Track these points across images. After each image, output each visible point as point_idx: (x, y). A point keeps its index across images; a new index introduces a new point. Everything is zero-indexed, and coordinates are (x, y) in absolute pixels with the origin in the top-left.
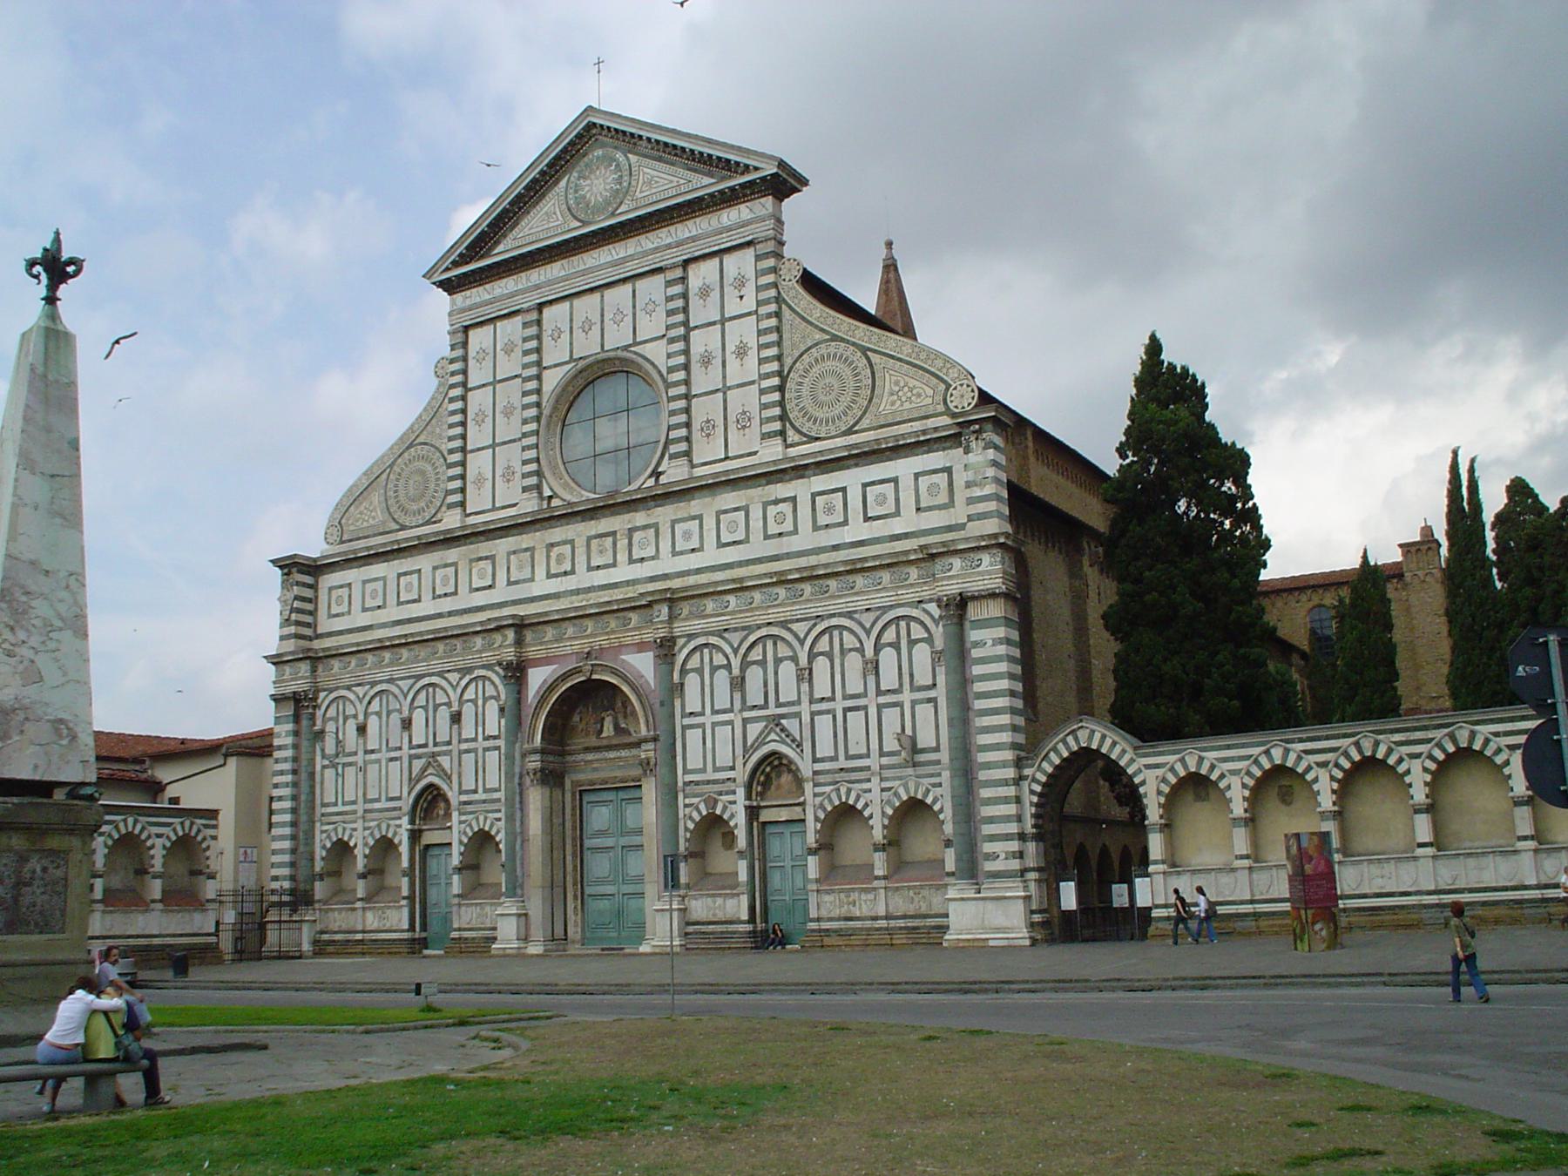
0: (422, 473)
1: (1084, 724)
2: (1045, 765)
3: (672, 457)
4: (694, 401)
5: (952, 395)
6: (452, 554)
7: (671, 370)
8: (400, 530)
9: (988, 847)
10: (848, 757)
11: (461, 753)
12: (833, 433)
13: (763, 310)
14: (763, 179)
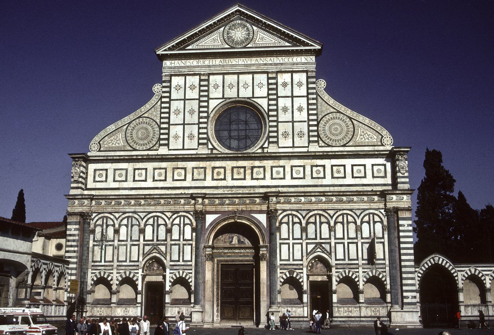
0: (147, 129)
1: (437, 255)
2: (423, 268)
3: (269, 143)
4: (279, 124)
5: (384, 140)
6: (164, 165)
9: (405, 294)
10: (349, 260)
11: (172, 245)
12: (338, 145)
13: (310, 96)
14: (315, 50)
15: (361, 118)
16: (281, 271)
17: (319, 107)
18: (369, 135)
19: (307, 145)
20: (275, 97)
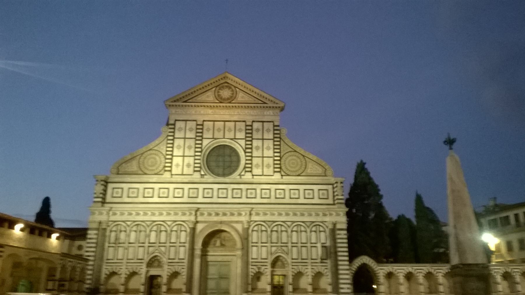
0: (155, 159)
3: (246, 171)
4: (253, 158)
7: (246, 148)
8: (143, 174)
9: (342, 286)
14: (279, 107)
15: (311, 156)
16: (253, 267)
17: (282, 147)
18: (316, 168)
19: (273, 174)
20: (250, 139)
